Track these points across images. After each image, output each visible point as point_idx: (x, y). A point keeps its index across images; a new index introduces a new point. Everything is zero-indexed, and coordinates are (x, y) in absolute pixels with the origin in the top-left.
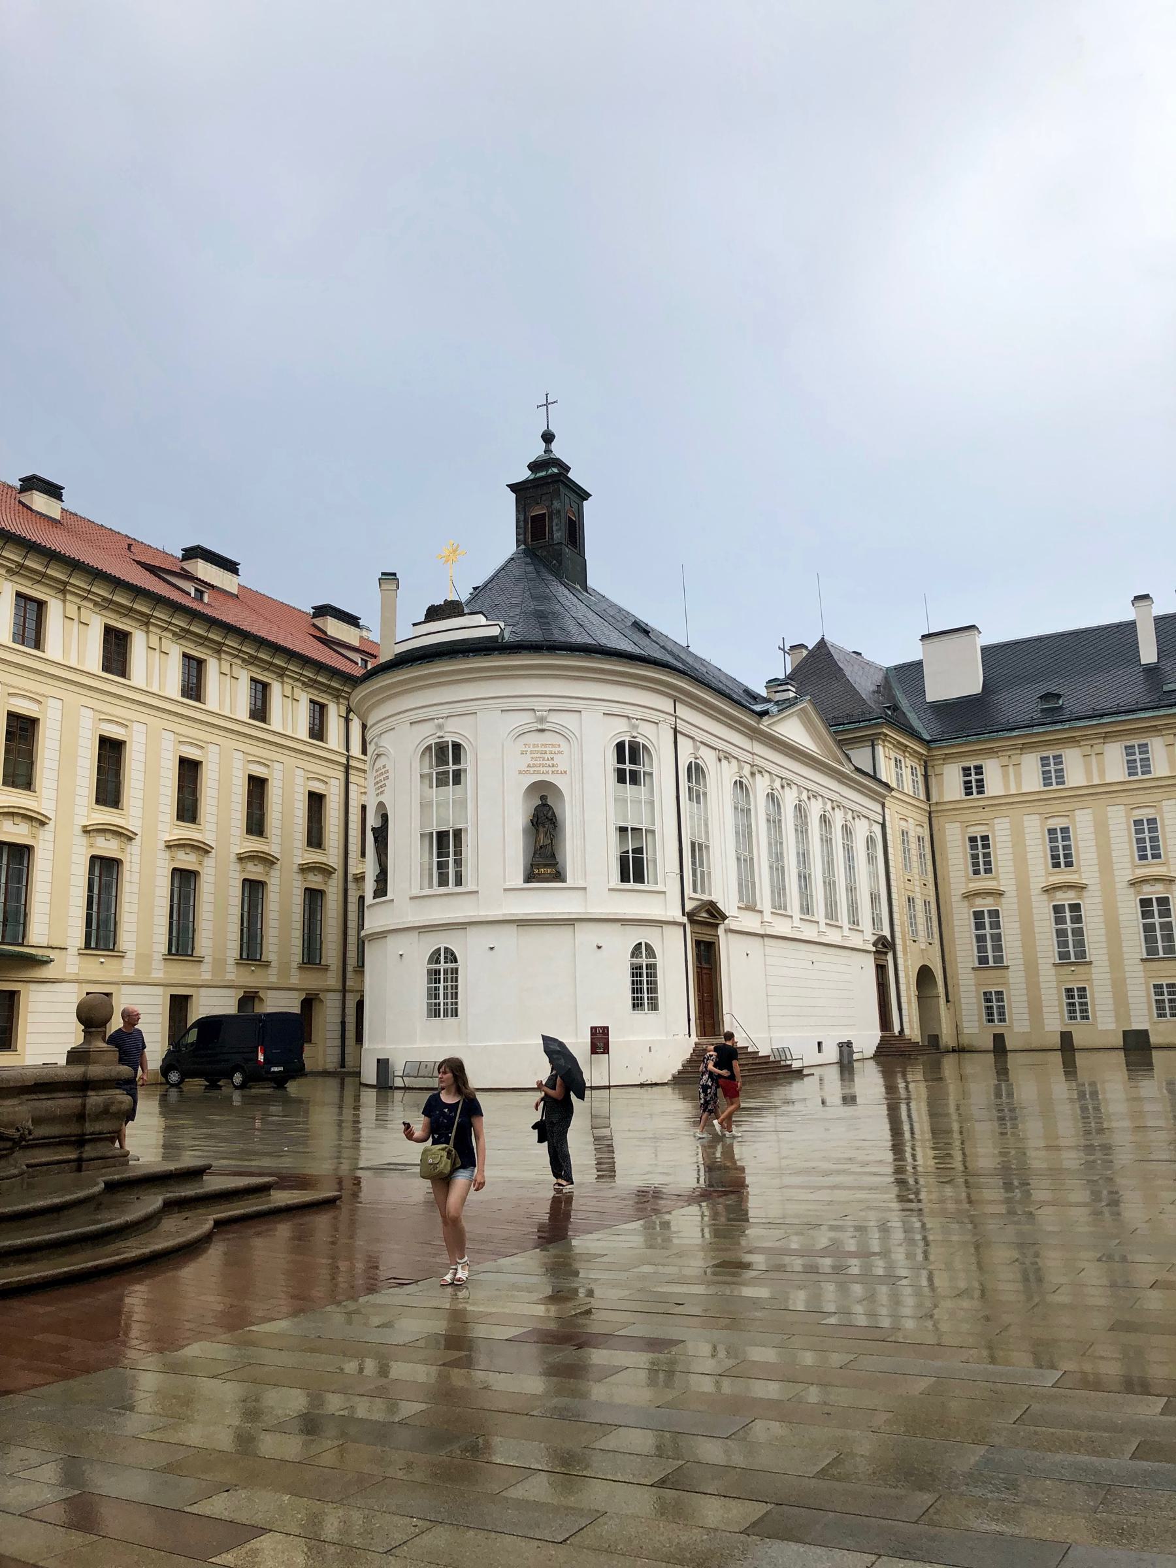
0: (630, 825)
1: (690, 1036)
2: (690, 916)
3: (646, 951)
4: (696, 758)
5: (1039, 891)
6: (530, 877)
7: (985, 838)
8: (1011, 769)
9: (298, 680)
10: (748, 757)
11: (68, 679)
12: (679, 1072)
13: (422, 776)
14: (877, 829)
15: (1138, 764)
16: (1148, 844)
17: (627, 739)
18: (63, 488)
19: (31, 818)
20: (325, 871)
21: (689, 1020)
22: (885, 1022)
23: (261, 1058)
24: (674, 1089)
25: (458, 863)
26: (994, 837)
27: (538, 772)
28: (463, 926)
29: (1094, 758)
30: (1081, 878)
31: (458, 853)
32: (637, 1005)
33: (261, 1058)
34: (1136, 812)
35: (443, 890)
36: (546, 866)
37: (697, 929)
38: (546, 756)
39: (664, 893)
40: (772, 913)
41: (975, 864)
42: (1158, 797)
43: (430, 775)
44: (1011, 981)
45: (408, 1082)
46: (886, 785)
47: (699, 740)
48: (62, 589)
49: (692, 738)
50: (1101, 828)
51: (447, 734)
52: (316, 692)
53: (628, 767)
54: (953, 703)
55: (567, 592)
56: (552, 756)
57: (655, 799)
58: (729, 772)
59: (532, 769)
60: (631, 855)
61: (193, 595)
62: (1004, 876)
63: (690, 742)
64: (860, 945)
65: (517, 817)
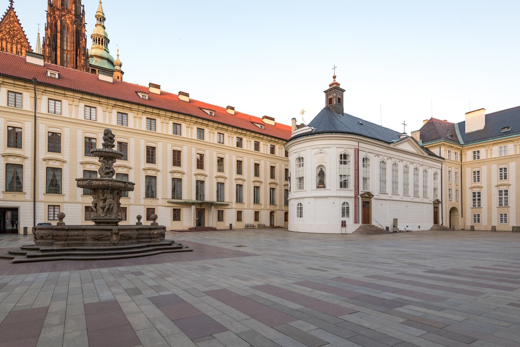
3: (346, 204)
4: (366, 156)
6: (318, 187)
7: (478, 172)
9: (282, 144)
12: (354, 231)
14: (439, 171)
17: (343, 153)
22: (436, 221)
30: (509, 183)
35: (300, 190)
36: (321, 185)
37: (363, 198)
40: (392, 194)
41: (475, 179)
43: (297, 165)
46: (443, 159)
53: (343, 160)
60: (343, 181)
64: (429, 202)
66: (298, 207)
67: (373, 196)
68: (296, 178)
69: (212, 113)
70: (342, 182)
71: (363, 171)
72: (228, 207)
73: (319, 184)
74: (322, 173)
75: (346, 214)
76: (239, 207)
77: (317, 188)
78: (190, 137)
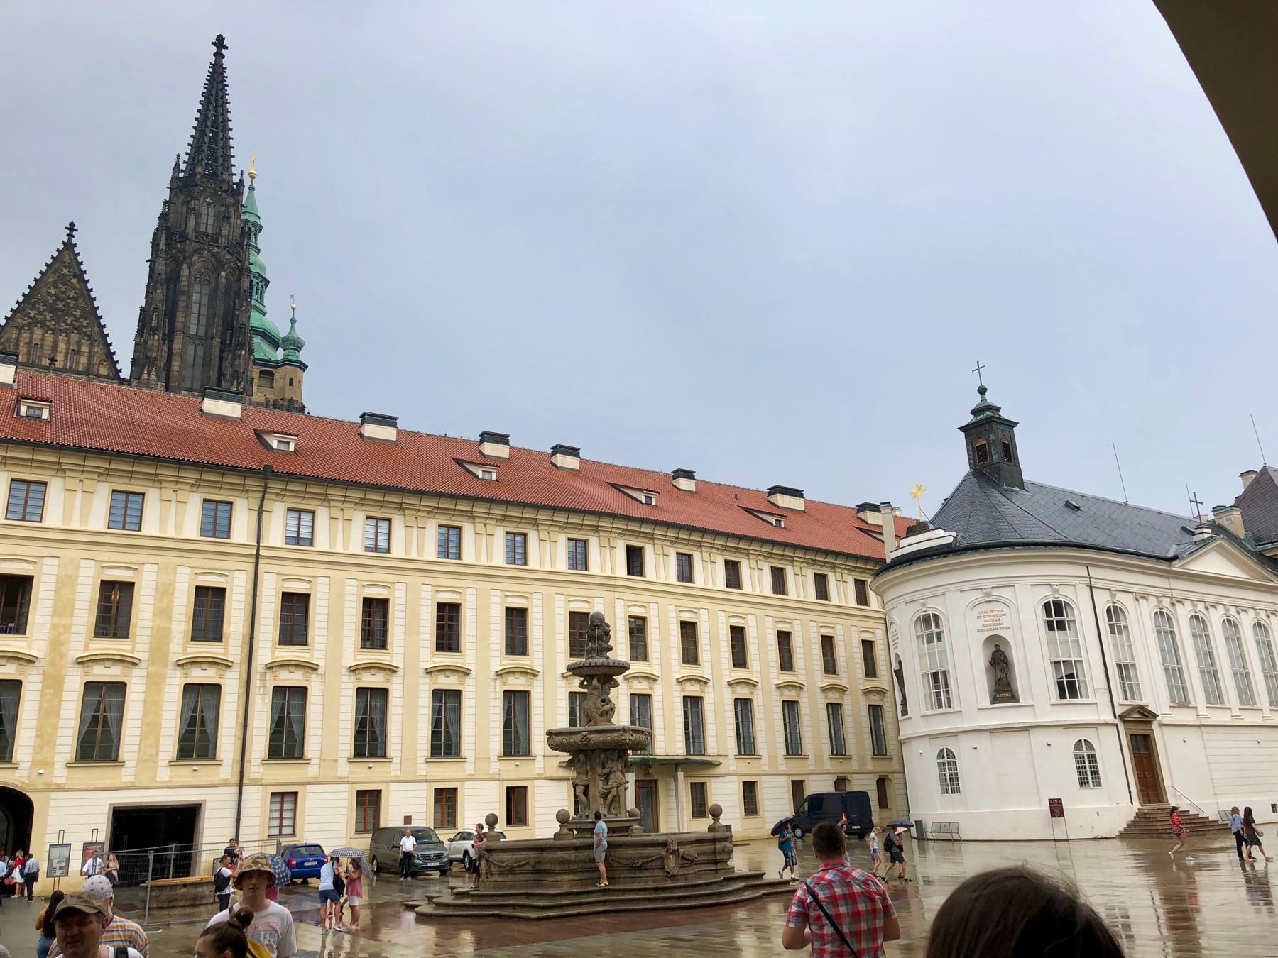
0: (1061, 659)
1: (1132, 803)
2: (1121, 717)
6: (995, 700)
9: (844, 569)
10: (1167, 593)
11: (709, 596)
17: (1051, 600)
18: (694, 472)
19: (700, 681)
20: (880, 692)
21: (1130, 792)
24: (1121, 842)
27: (991, 630)
28: (955, 734)
31: (947, 686)
32: (1083, 783)
35: (940, 711)
36: (1004, 692)
37: (1130, 726)
39: (1096, 703)
45: (936, 836)
47: (1115, 589)
48: (699, 545)
49: (1109, 589)
51: (928, 609)
52: (858, 574)
53: (1054, 619)
55: (1002, 499)
57: (1079, 638)
58: (1147, 609)
60: (1065, 679)
61: (774, 524)
63: (1107, 592)
65: (980, 661)
66: (942, 761)
67: (1155, 716)
69: (651, 498)
70: (1063, 681)
71: (1115, 645)
72: (719, 771)
73: (996, 692)
74: (1002, 658)
75: (1089, 776)
76: (747, 768)
77: (992, 703)
78: (608, 573)
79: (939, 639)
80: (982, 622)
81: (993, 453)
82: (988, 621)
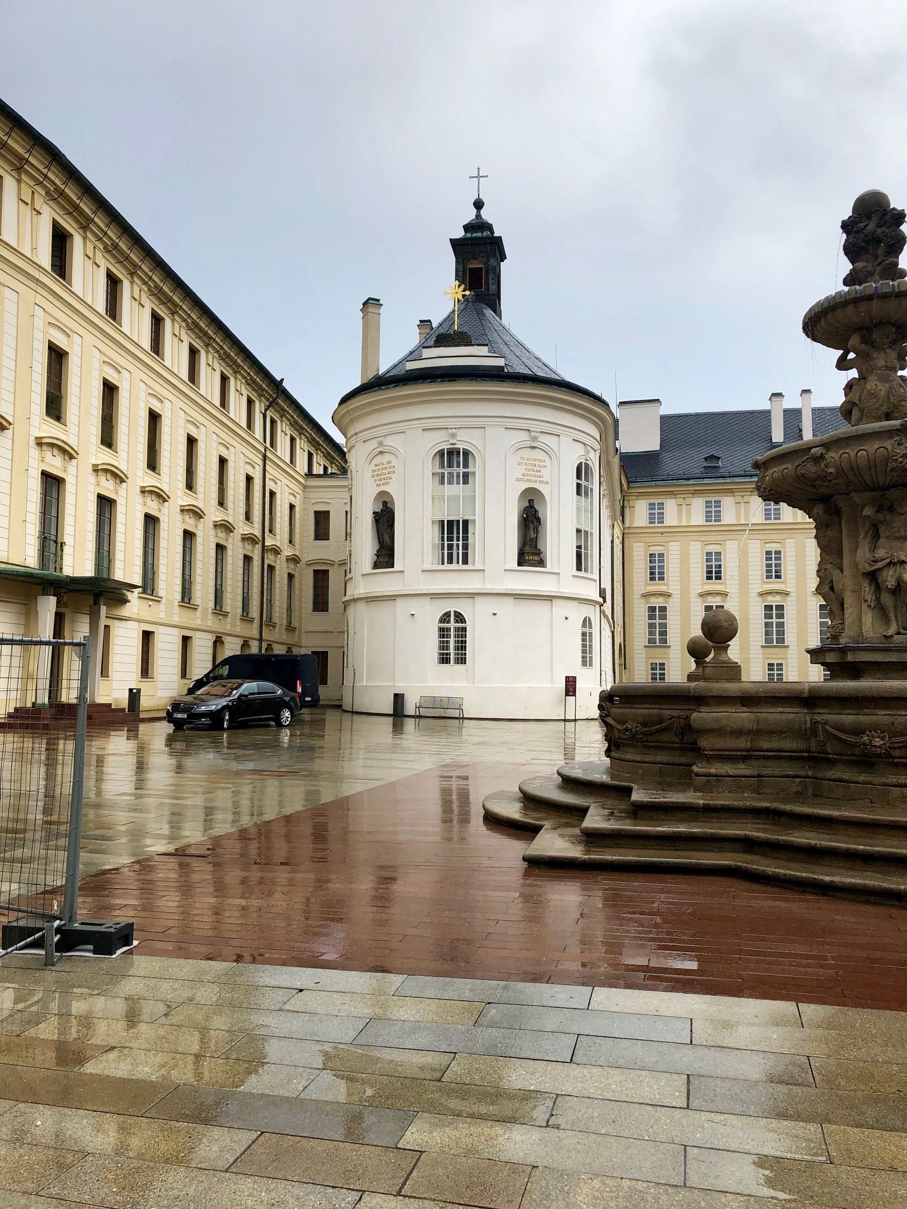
0: (583, 528)
5: (696, 595)
8: (684, 507)
13: (433, 474)
15: (772, 512)
16: (774, 568)
17: (584, 461)
23: (300, 690)
25: (465, 547)
26: (668, 555)
27: (530, 481)
28: (472, 595)
29: (742, 505)
30: (726, 588)
31: (466, 538)
33: (300, 690)
34: (767, 545)
36: (533, 554)
38: (536, 468)
42: (784, 536)
44: (671, 656)
50: (743, 555)
51: (459, 442)
54: (639, 455)
56: (540, 469)
59: (526, 478)
62: (672, 583)
68: (433, 522)
79: (466, 482)
80: (522, 470)
81: (490, 281)
82: (529, 470)
